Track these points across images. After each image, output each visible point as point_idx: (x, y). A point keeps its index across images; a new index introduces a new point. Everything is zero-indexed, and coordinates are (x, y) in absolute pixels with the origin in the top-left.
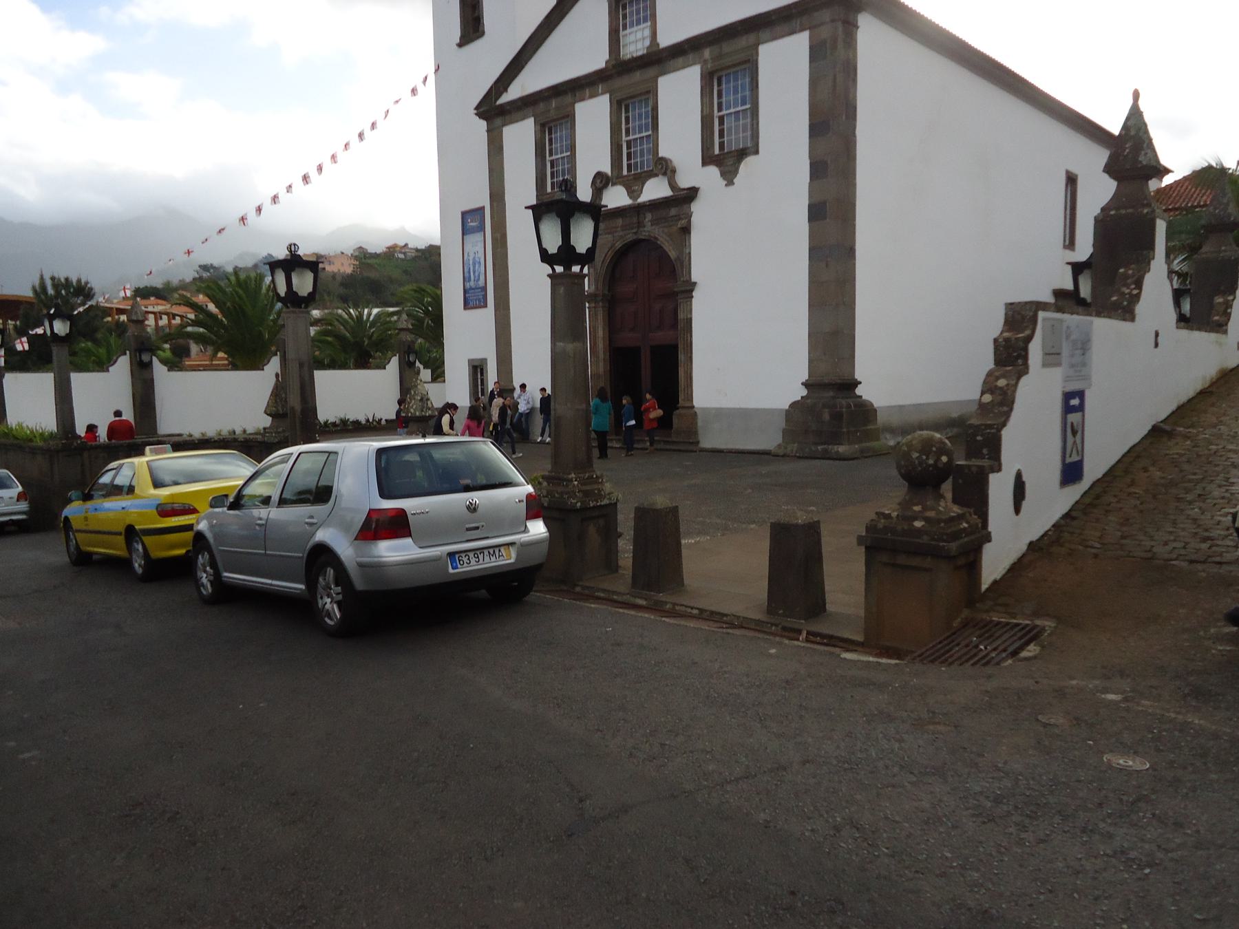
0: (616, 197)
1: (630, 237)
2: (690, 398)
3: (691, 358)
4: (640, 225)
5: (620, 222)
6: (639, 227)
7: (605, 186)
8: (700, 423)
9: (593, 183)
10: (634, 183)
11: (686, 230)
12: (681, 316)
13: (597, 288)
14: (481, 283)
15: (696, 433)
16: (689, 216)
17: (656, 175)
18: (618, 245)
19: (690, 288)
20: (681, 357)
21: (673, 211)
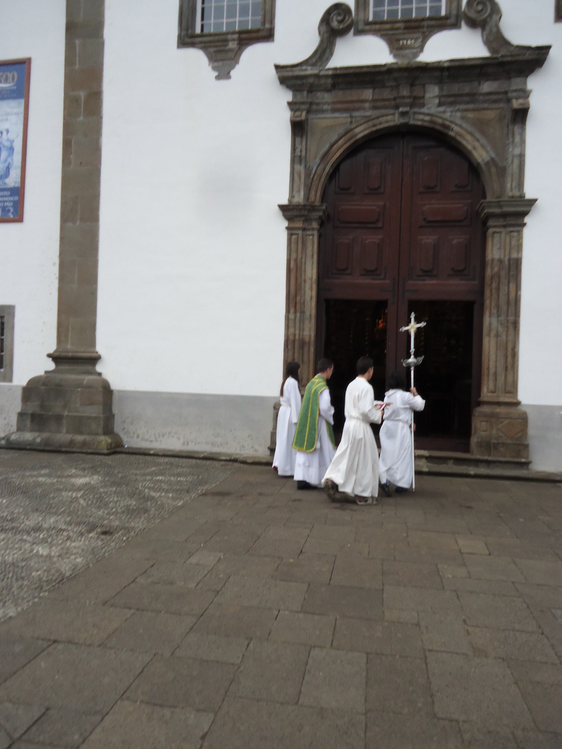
0: (366, 51)
1: (392, 119)
2: (513, 388)
3: (516, 325)
4: (417, 101)
5: (368, 94)
6: (412, 106)
7: (343, 32)
8: (531, 431)
9: (326, 19)
10: (408, 30)
11: (521, 115)
12: (494, 251)
13: (307, 197)
14: (13, 180)
15: (526, 446)
16: (525, 94)
17: (456, 26)
18: (361, 132)
19: (518, 211)
20: (490, 321)
21: (487, 87)
